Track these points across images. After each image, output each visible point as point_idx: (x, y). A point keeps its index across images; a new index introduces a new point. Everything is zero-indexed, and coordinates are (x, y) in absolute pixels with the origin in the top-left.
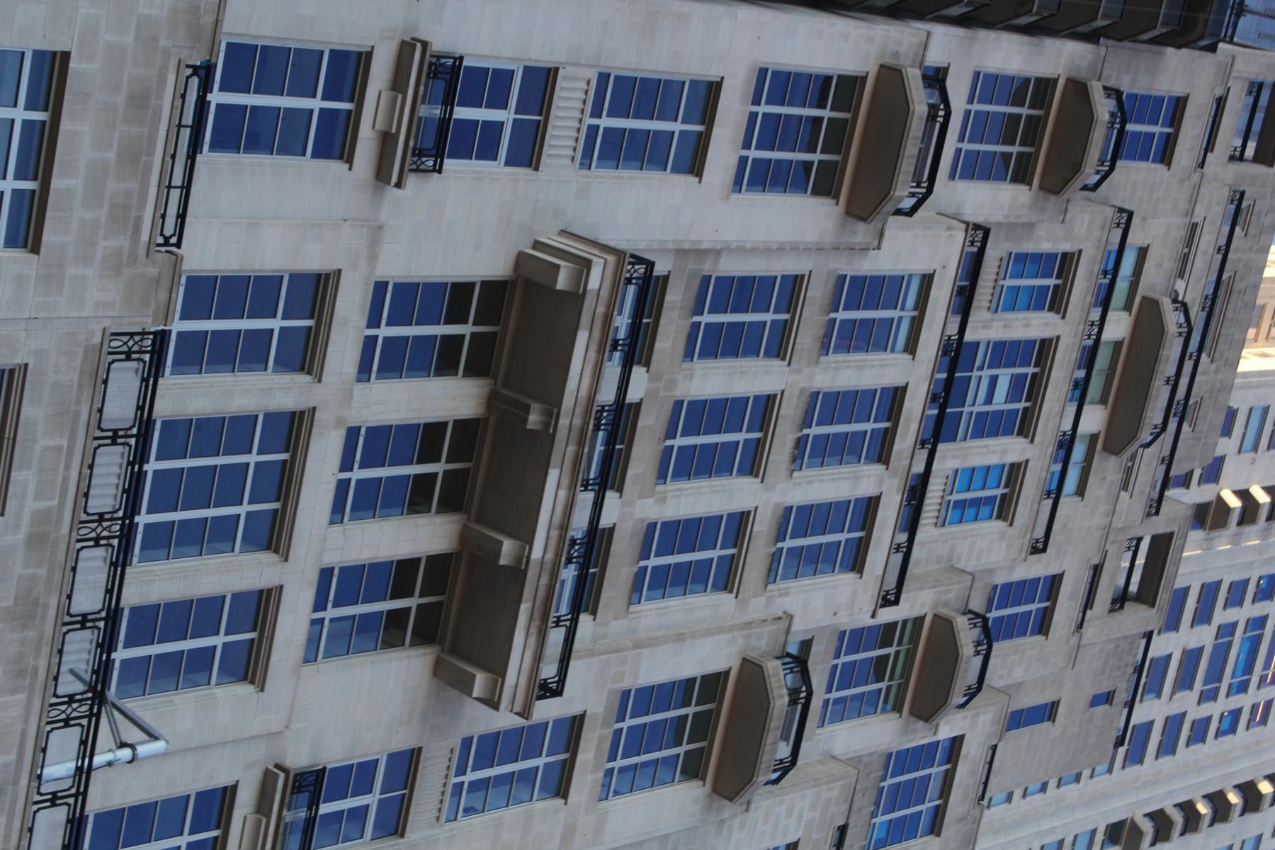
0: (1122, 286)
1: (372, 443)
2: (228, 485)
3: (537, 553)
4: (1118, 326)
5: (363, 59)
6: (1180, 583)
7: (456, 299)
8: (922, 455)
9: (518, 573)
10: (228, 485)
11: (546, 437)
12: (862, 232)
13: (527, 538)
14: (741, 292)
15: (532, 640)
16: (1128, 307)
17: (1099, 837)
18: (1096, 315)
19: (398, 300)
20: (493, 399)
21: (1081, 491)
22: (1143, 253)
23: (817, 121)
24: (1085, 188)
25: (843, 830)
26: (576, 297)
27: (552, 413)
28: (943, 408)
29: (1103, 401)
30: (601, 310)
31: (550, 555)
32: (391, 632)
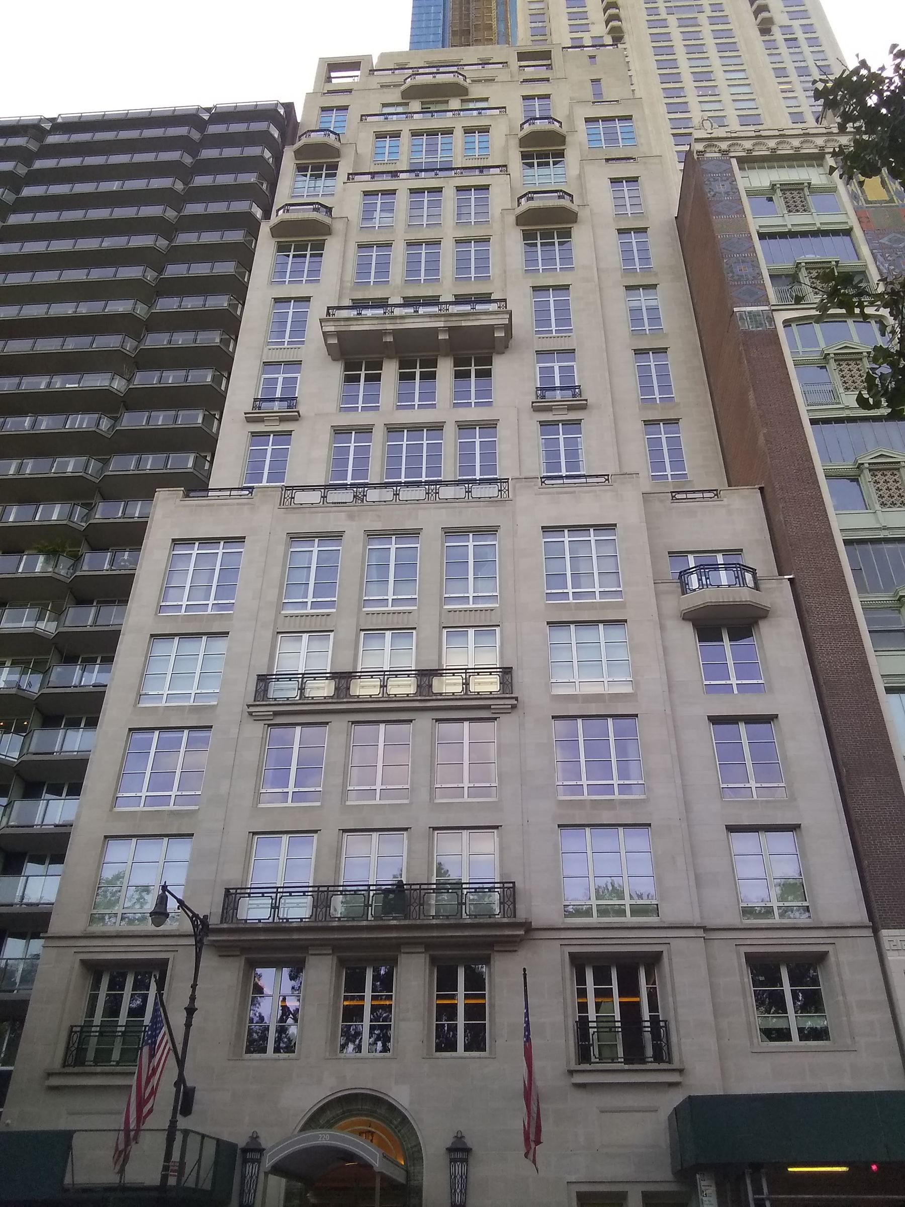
0: (400, 109)
1: (404, 397)
2: (415, 450)
3: (442, 324)
4: (415, 106)
5: (254, 434)
6: (530, 43)
7: (350, 379)
8: (492, 171)
9: (451, 330)
10: (415, 450)
11: (395, 332)
12: (338, 226)
13: (436, 330)
14: (363, 269)
15: (478, 317)
16: (407, 104)
17: (767, 38)
18: (450, 114)
19: (347, 402)
20: (390, 358)
21: (486, 100)
22: (384, 105)
23: (542, 244)
24: (561, 126)
25: (607, 160)
26: (339, 334)
27: (384, 332)
28: (421, 171)
29: (447, 102)
30: (343, 323)
31: (443, 319)
32: (485, 374)
